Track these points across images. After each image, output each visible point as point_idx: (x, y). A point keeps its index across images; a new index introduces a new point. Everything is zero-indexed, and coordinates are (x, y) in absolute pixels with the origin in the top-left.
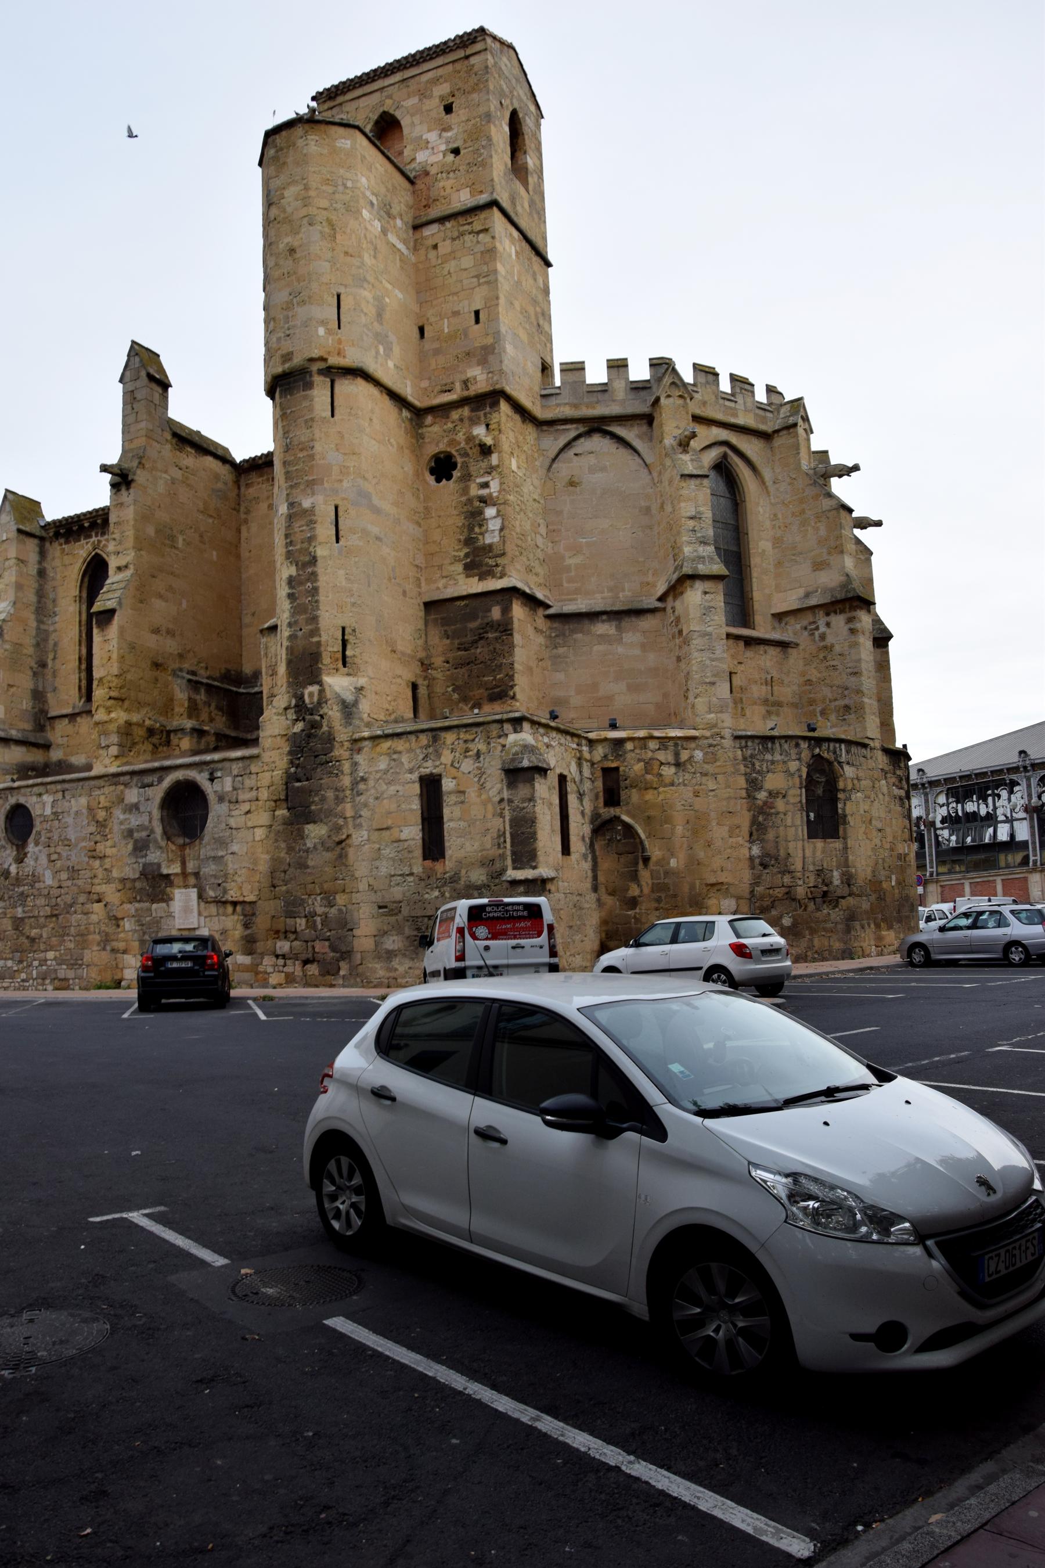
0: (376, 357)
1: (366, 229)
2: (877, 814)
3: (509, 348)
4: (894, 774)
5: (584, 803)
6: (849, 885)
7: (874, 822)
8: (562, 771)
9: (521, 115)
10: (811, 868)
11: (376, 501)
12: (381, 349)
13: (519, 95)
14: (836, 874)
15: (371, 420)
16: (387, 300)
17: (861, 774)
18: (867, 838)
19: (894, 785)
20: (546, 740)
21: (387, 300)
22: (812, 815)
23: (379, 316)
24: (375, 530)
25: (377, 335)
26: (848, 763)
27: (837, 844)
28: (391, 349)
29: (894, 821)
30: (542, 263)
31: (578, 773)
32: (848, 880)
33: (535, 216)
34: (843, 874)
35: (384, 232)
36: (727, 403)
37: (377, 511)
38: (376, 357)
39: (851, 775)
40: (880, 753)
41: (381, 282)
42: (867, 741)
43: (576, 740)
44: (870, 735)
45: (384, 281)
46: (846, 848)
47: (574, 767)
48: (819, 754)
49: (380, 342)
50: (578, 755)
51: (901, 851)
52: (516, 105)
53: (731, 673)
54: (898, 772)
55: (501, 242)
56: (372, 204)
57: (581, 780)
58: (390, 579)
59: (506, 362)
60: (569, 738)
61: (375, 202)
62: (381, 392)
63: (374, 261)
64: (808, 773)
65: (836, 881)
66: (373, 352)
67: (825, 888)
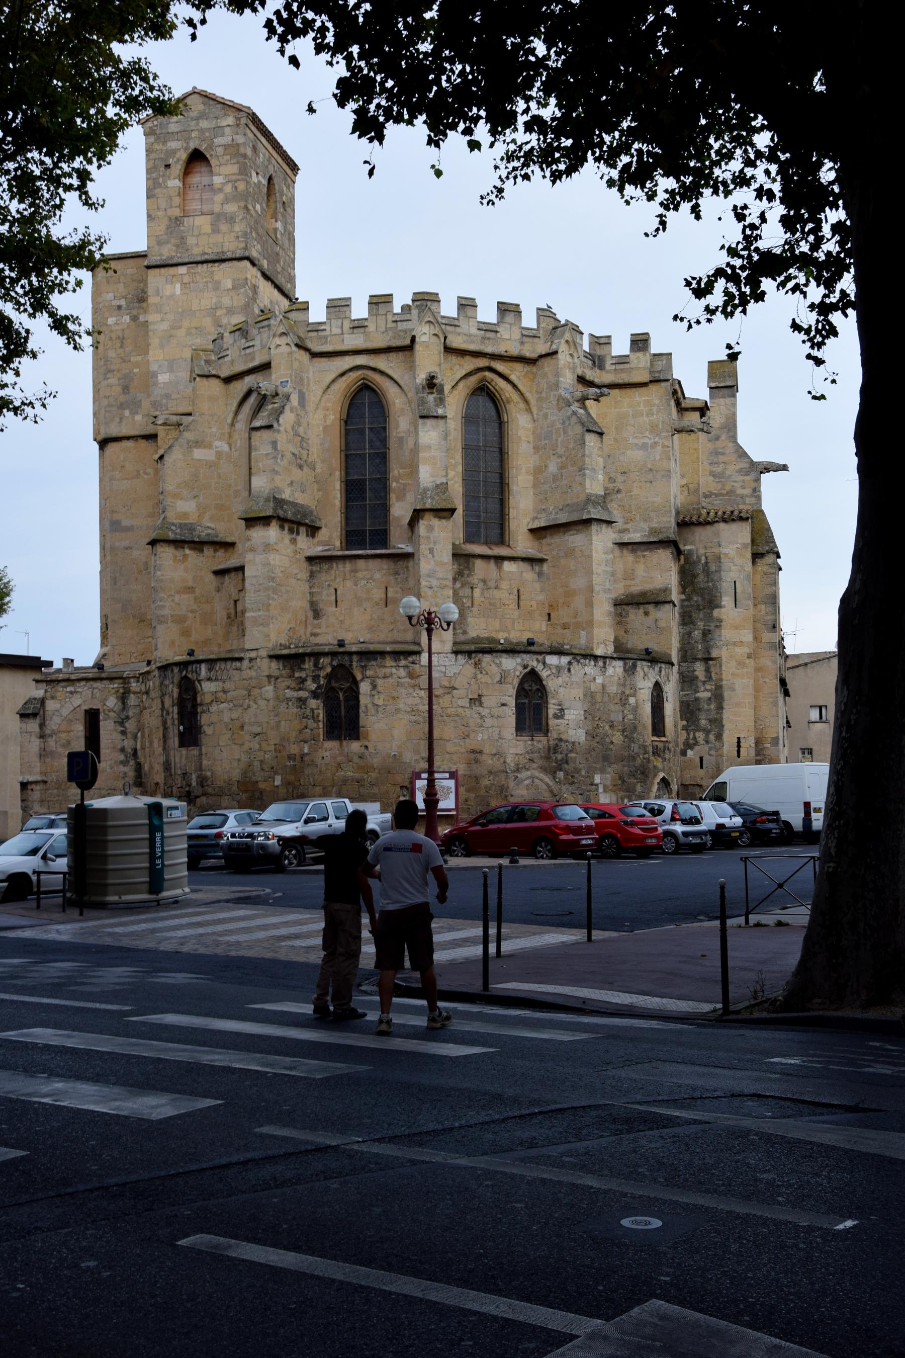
0: (120, 422)
1: (112, 331)
2: (253, 720)
3: (163, 378)
4: (291, 676)
5: (127, 725)
6: (203, 787)
7: (246, 728)
8: (91, 707)
9: (202, 148)
10: (179, 772)
11: (126, 523)
12: (127, 413)
13: (202, 131)
14: (194, 776)
15: (123, 467)
16: (136, 370)
17: (228, 685)
18: (236, 744)
19: (288, 687)
20: (69, 689)
21: (136, 370)
22: (181, 728)
23: (126, 389)
24: (126, 543)
25: (122, 406)
26: (209, 679)
27: (194, 751)
28: (140, 406)
29: (283, 723)
30: (235, 263)
31: (120, 704)
32: (202, 781)
33: (224, 227)
34: (198, 777)
35: (135, 318)
36: (248, 351)
37: (129, 529)
38: (120, 422)
39: (213, 689)
40: (266, 661)
41: (129, 361)
42: (242, 655)
43: (121, 681)
44: (248, 646)
45: (132, 359)
46: (201, 754)
47: (112, 702)
48: (186, 676)
49: (124, 409)
50: (121, 691)
51: (293, 752)
52: (192, 146)
53: (235, 601)
54: (297, 675)
55: (157, 293)
56: (119, 307)
57: (124, 709)
58: (140, 572)
59: (155, 393)
60: (104, 682)
61: (123, 302)
62: (136, 440)
63: (120, 351)
64: (180, 694)
65: (194, 784)
66: (118, 420)
67: (187, 789)
